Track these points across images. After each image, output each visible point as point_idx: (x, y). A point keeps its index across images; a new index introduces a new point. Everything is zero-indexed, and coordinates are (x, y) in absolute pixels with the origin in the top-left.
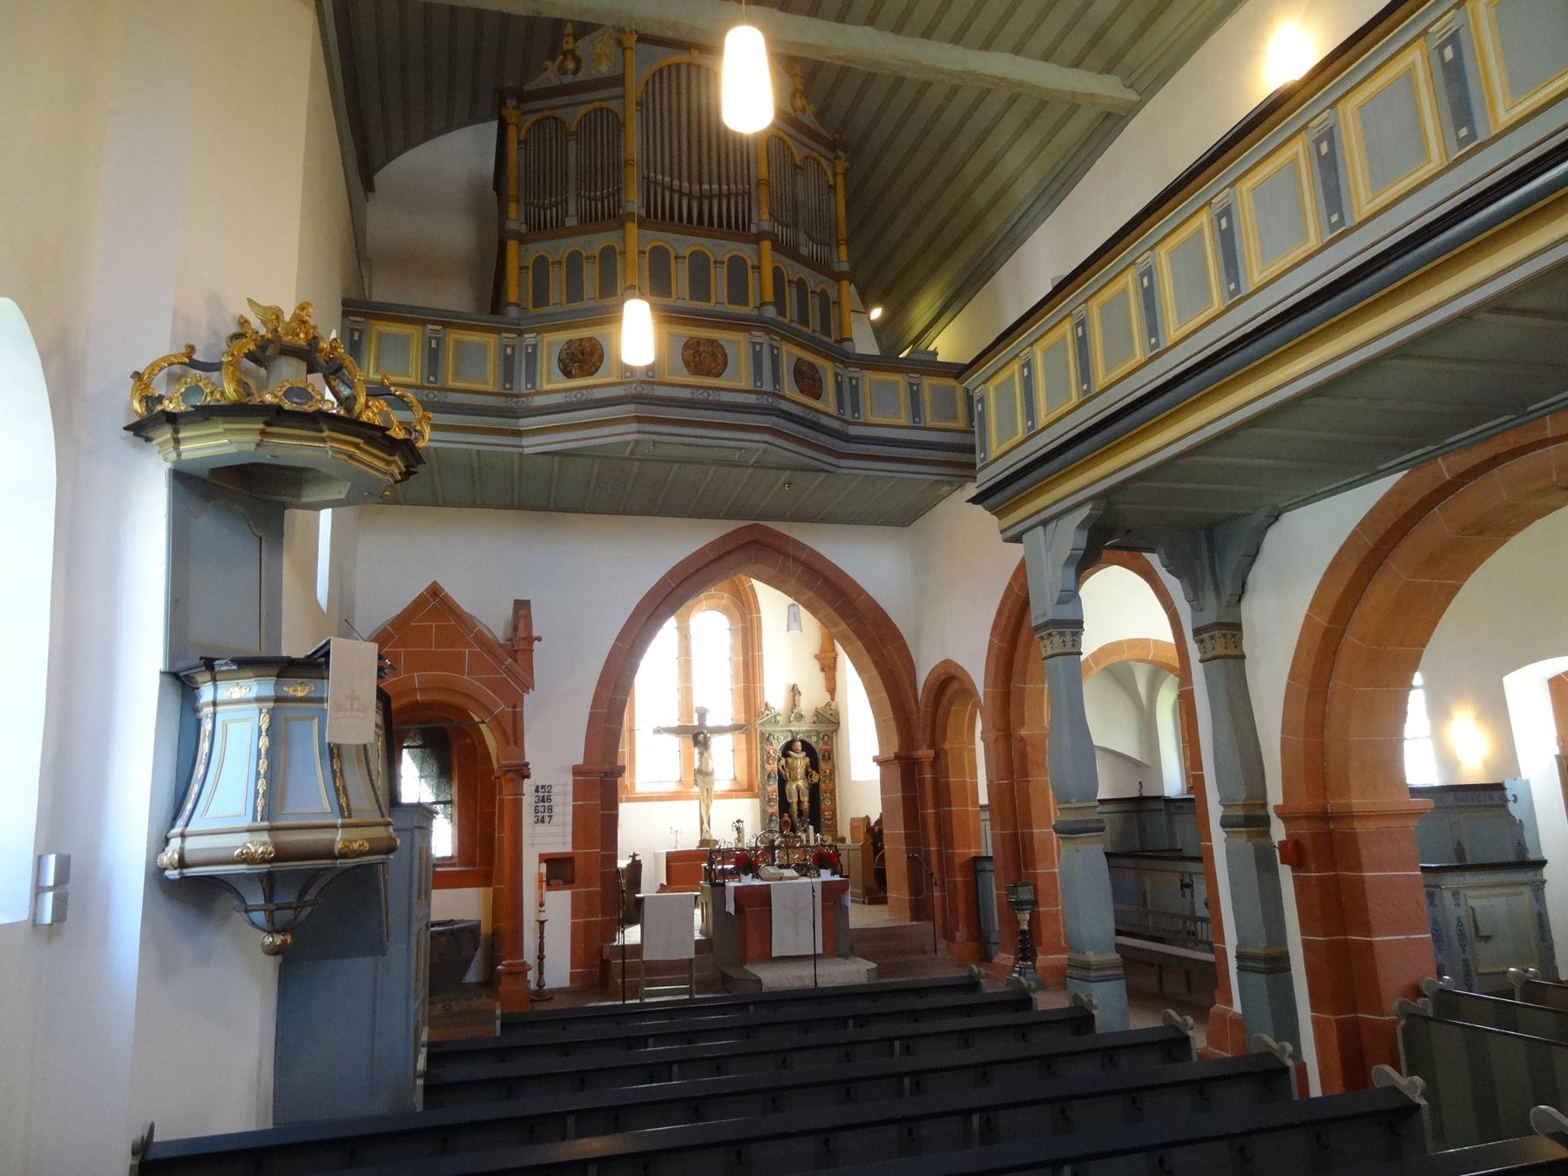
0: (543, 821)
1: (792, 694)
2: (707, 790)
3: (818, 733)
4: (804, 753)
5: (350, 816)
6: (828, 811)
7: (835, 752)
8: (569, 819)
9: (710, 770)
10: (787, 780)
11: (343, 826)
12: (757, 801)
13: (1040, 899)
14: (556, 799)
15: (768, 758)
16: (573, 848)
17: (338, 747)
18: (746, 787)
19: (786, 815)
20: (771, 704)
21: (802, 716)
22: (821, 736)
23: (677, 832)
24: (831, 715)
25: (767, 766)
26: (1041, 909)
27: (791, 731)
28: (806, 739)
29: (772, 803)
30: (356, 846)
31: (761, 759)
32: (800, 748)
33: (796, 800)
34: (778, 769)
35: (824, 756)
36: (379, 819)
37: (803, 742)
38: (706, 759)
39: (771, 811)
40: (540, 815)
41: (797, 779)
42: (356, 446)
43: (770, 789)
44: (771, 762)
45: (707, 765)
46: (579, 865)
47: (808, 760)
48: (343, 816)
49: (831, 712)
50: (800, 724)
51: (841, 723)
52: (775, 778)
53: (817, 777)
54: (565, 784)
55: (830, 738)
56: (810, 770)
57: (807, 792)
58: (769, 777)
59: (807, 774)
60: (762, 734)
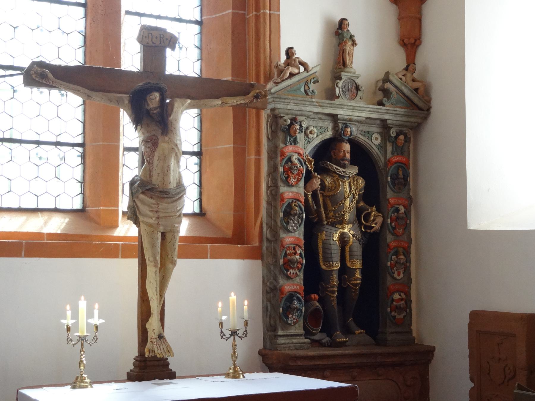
1: (335, 41)
2: (163, 234)
3: (384, 126)
4: (353, 170)
6: (398, 291)
7: (411, 171)
9: (173, 184)
10: (320, 221)
12: (256, 265)
15: (288, 171)
18: (229, 233)
19: (317, 297)
20: (300, 54)
21: (357, 88)
22: (393, 133)
23: (82, 339)
24: (416, 90)
25: (283, 189)
27: (334, 118)
28: (362, 139)
29: (291, 272)
31: (269, 174)
32: (348, 156)
33: (337, 266)
34: (306, 195)
35: (395, 178)
37: (355, 144)
38: (165, 159)
39: (288, 287)
41: (342, 222)
43: (288, 239)
44: (292, 180)
45: (165, 171)
47: (361, 182)
49: (416, 85)
50: (353, 103)
51: (432, 110)
52: (300, 215)
53: (379, 220)
55: (407, 140)
56: (362, 204)
57: (358, 250)
58: (288, 213)
59: (359, 212)
60: (275, 117)
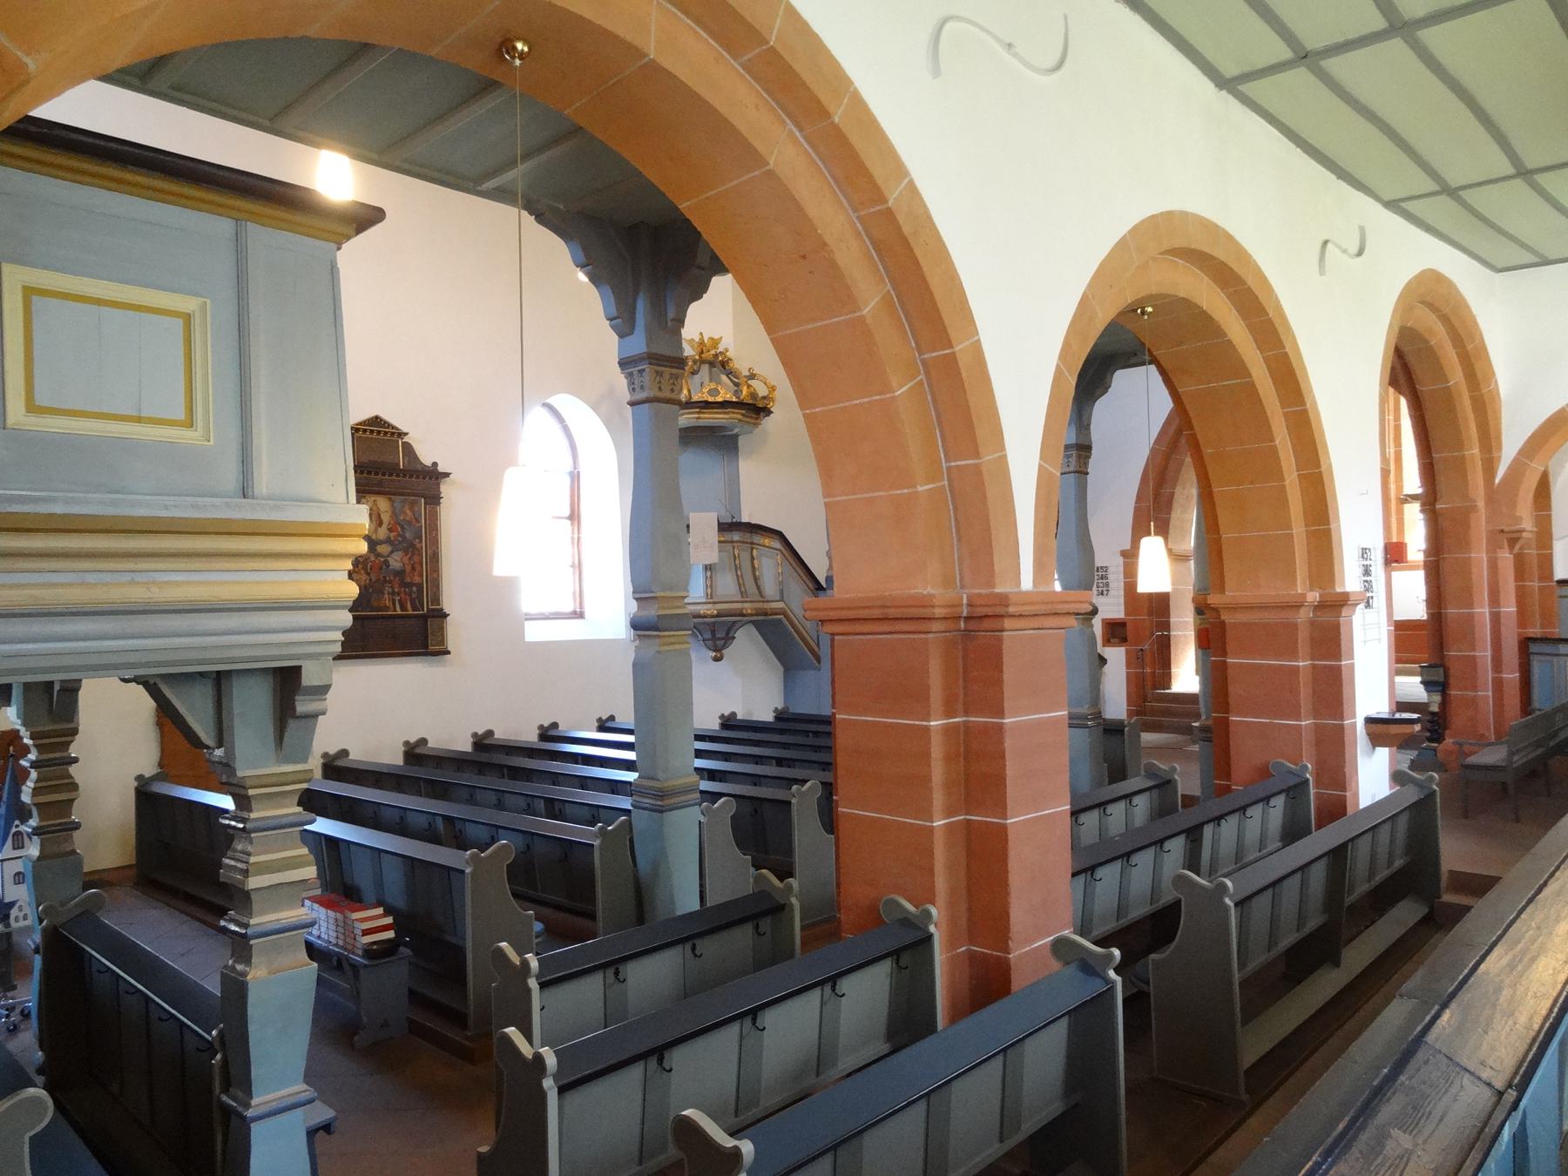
0: (1102, 594)
5: (711, 598)
8: (1122, 593)
11: (706, 603)
13: (1452, 681)
14: (1111, 577)
16: (1126, 614)
17: (710, 565)
26: (1453, 693)
30: (709, 612)
36: (740, 599)
40: (1100, 589)
42: (698, 413)
46: (1129, 627)
48: (707, 598)
54: (1118, 566)
